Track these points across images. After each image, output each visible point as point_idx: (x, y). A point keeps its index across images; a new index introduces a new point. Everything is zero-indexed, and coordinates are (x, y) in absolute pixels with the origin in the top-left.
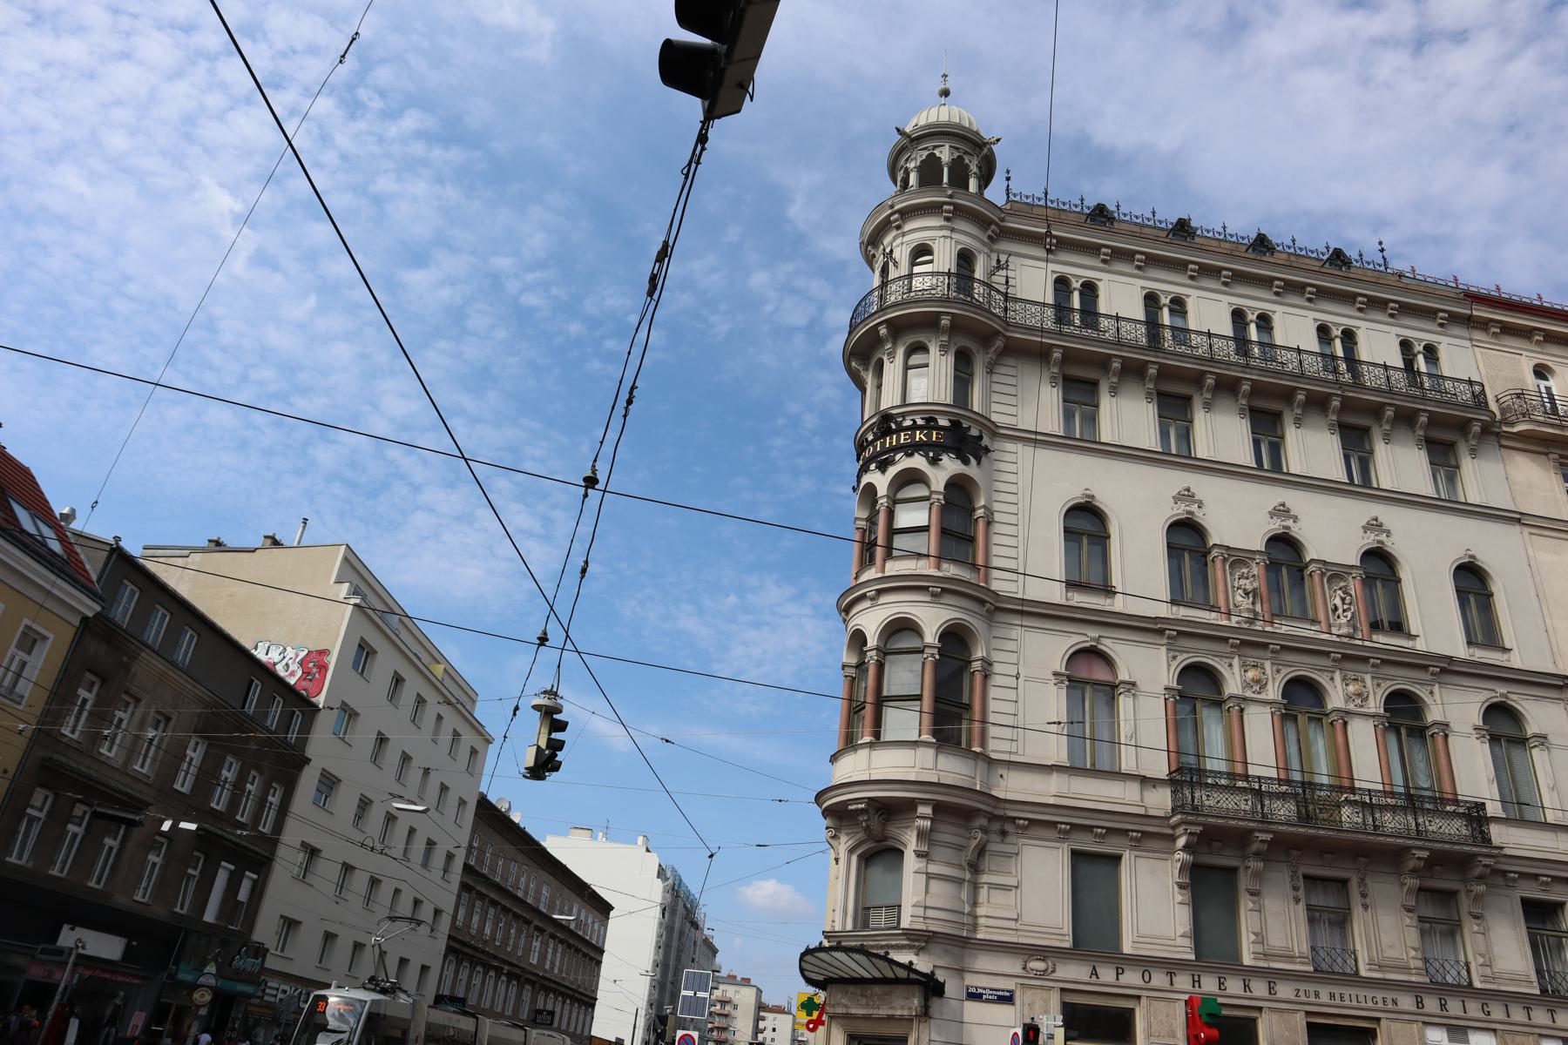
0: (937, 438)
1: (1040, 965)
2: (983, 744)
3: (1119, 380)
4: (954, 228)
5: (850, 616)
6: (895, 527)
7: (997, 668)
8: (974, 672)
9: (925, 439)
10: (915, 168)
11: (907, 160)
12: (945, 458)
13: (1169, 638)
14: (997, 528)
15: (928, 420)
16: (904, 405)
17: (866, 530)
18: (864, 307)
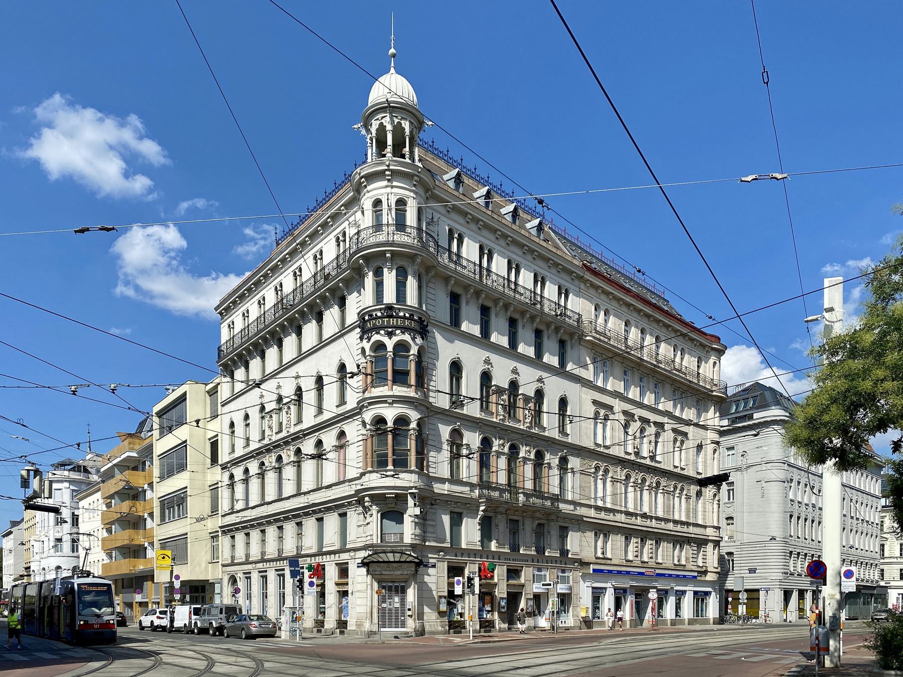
2: (428, 470)
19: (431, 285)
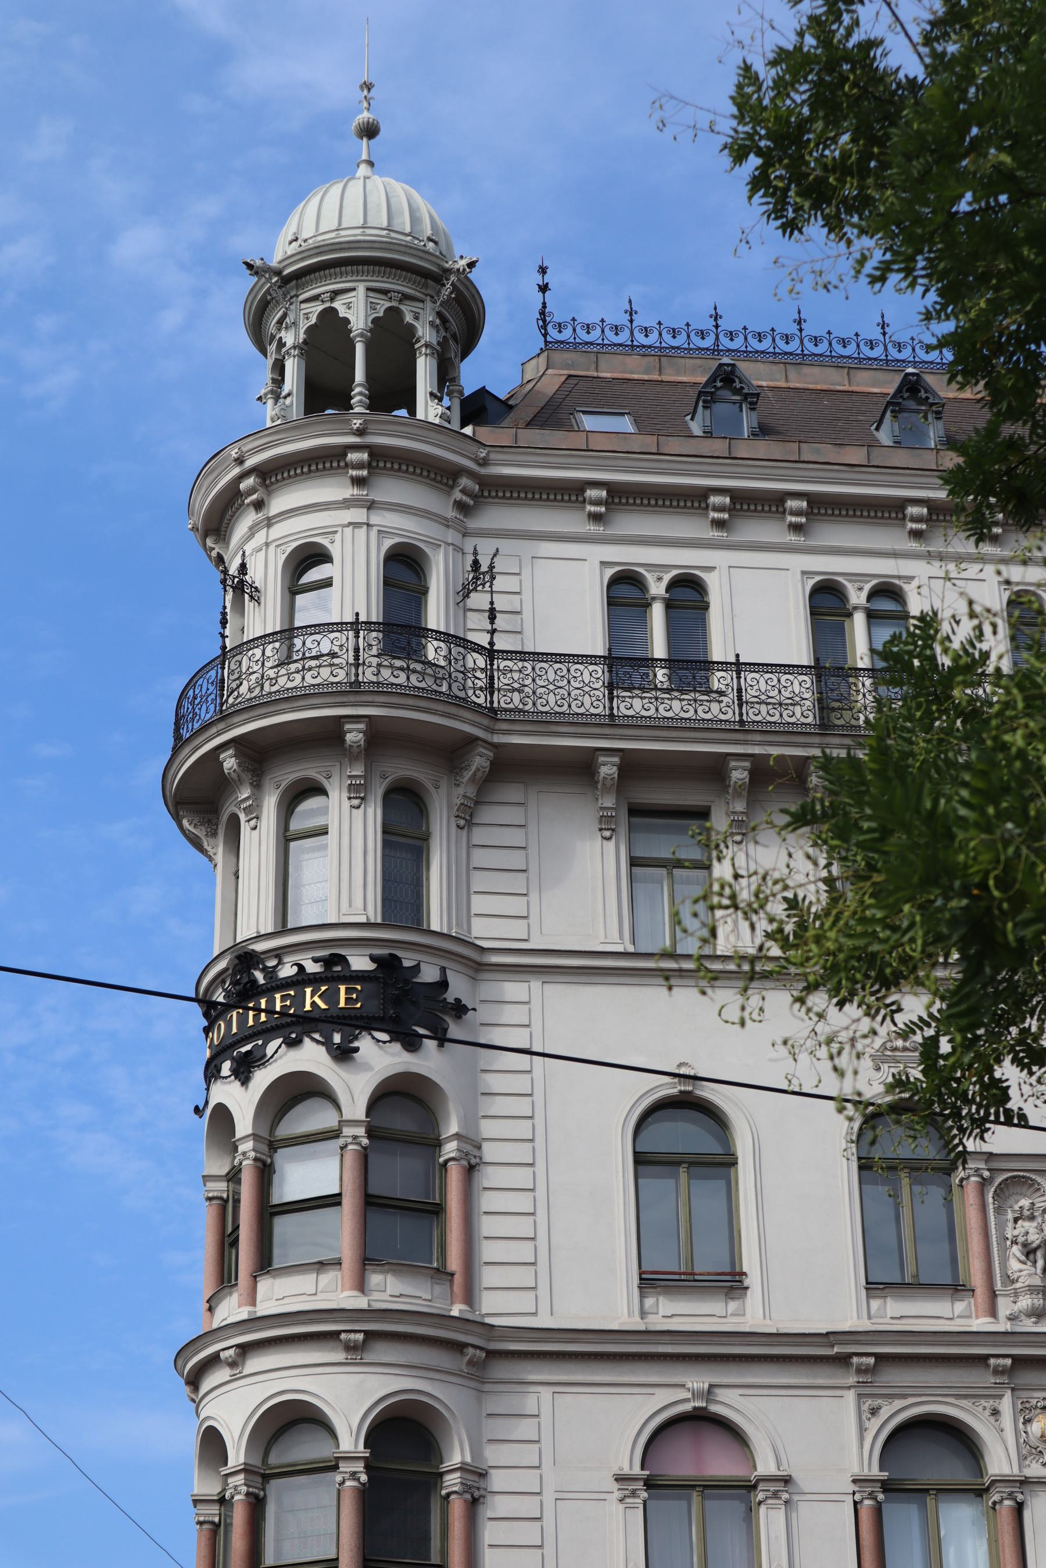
0: (348, 1000)
3: (750, 804)
4: (373, 502)
5: (200, 1395)
6: (276, 1200)
7: (498, 1481)
8: (449, 1495)
9: (323, 1006)
10: (294, 347)
11: (280, 322)
12: (365, 1044)
13: (860, 1371)
14: (490, 1177)
15: (329, 962)
16: (283, 929)
17: (226, 1201)
18: (192, 703)
19: (488, 814)
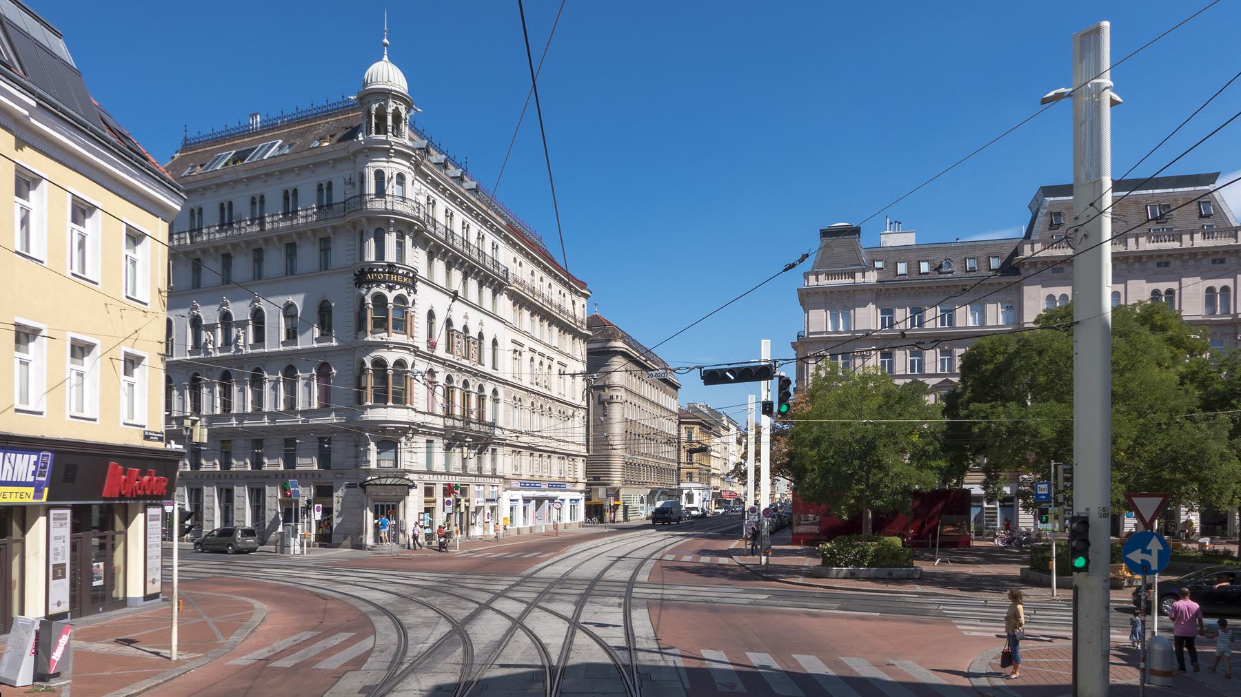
1: (421, 476)
